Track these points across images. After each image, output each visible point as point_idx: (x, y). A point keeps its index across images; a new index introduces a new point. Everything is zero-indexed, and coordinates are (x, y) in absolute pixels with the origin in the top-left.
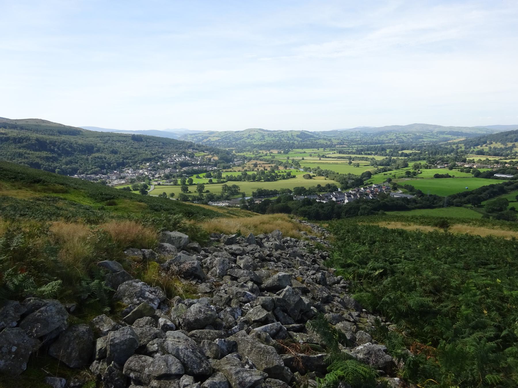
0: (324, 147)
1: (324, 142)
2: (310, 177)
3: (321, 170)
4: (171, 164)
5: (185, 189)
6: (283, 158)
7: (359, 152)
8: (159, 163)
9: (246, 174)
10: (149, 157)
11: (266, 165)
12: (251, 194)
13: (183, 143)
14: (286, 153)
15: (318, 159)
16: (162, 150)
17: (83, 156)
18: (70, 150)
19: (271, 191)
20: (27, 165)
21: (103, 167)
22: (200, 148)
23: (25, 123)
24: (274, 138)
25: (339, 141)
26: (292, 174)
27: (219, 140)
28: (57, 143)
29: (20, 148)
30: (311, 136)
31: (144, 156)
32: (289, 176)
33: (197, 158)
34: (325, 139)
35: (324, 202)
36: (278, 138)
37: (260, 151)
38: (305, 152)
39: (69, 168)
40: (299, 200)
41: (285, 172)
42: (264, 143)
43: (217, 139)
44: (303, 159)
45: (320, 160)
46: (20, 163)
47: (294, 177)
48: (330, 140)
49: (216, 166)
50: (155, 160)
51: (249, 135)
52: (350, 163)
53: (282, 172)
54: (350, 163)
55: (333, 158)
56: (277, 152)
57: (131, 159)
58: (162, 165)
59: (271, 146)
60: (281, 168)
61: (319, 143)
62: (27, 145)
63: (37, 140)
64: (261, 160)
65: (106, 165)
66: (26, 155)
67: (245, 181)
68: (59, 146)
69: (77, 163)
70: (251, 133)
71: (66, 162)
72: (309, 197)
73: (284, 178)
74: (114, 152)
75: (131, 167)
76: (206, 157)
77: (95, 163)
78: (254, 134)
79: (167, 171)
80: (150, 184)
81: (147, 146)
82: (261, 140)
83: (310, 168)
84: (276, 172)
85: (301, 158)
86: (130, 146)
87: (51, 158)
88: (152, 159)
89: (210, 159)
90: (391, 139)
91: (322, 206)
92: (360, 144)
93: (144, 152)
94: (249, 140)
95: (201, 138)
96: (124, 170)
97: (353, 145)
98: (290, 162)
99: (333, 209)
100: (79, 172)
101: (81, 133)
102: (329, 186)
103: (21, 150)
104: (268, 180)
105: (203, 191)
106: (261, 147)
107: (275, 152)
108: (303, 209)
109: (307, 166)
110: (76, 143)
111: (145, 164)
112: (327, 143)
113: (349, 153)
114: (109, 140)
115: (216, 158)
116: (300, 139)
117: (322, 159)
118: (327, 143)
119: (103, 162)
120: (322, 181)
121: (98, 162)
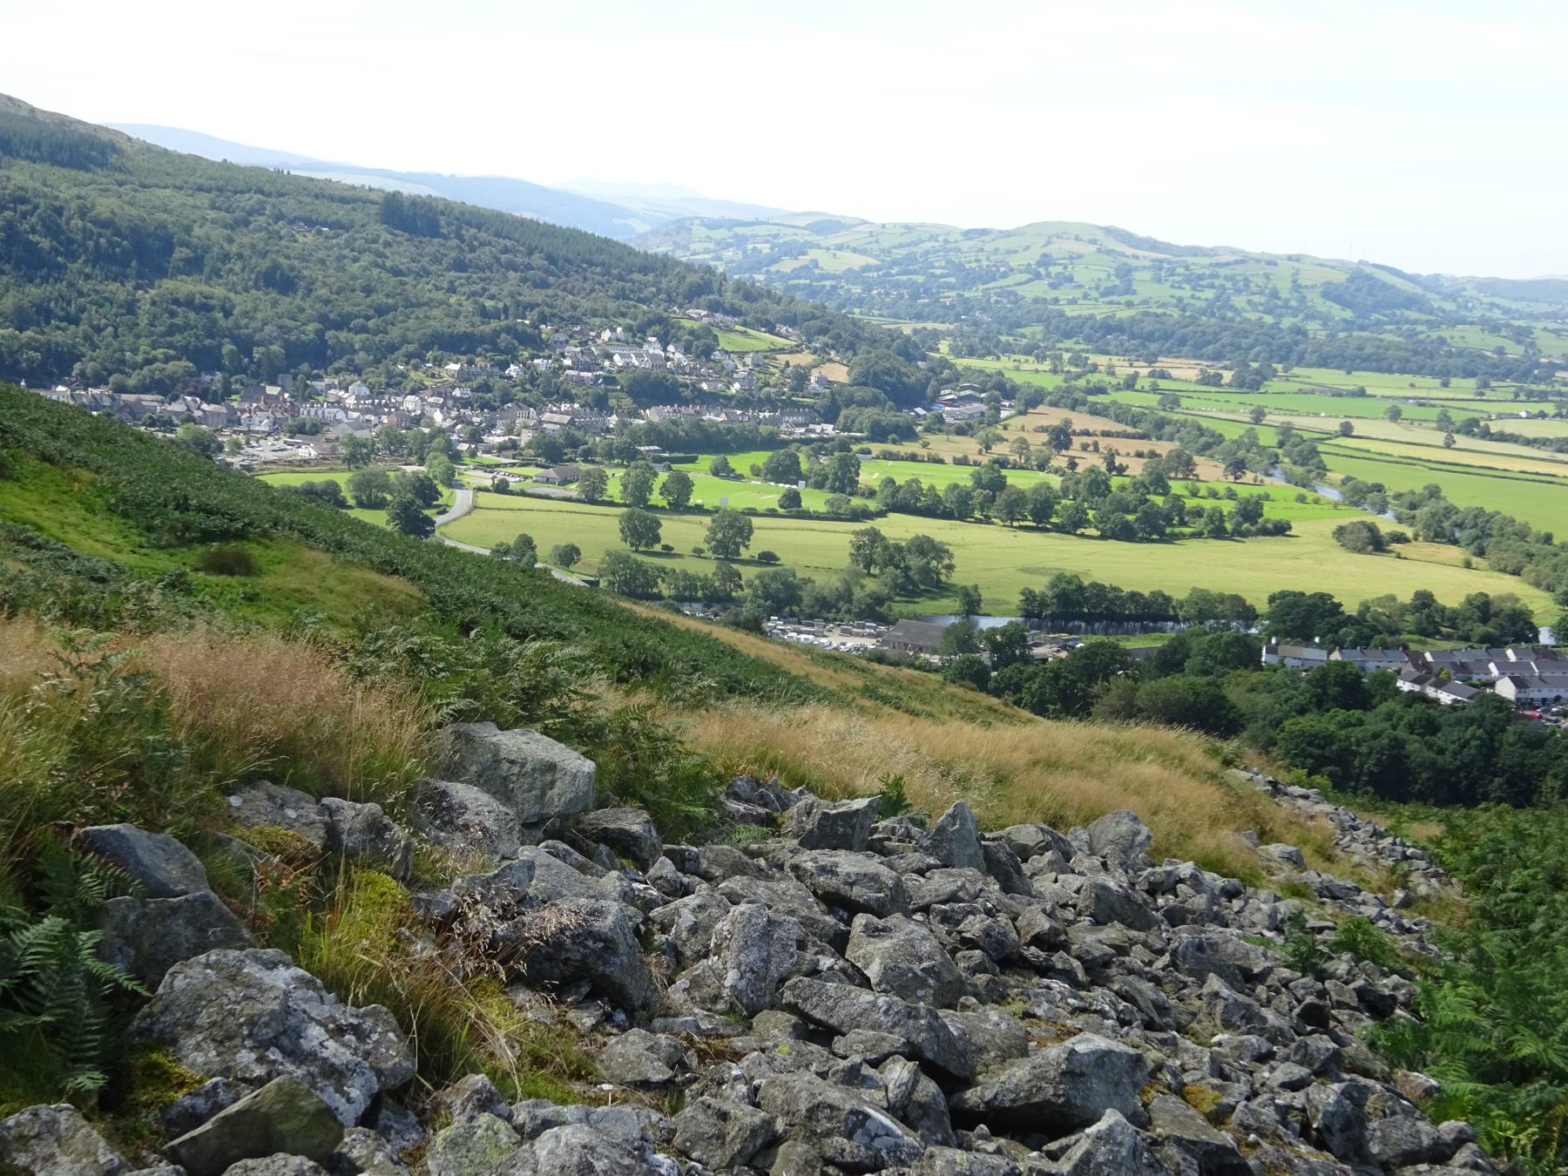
0: (1486, 371)
2: (1377, 543)
3: (1450, 511)
4: (580, 382)
5: (642, 531)
6: (1224, 414)
8: (513, 370)
9: (999, 485)
10: (462, 326)
11: (1125, 446)
12: (1016, 599)
13: (658, 266)
14: (1250, 383)
15: (1440, 438)
16: (539, 296)
17: (114, 286)
18: (45, 243)
19: (1134, 596)
21: (206, 359)
22: (751, 305)
24: (1186, 293)
26: (1271, 513)
27: (867, 268)
30: (1411, 302)
31: (437, 321)
32: (1251, 522)
33: (728, 363)
34: (1495, 329)
35: (1446, 698)
36: (1210, 294)
38: (1361, 393)
39: (28, 346)
40: (1294, 673)
41: (1231, 495)
42: (1123, 314)
43: (858, 261)
44: (1346, 431)
45: (1448, 446)
47: (1281, 529)
48: (1521, 335)
49: (830, 415)
50: (496, 349)
51: (1046, 261)
53: (1214, 495)
55: (1528, 442)
57: (363, 329)
58: (532, 380)
59: (1166, 336)
60: (1211, 472)
64: (1095, 411)
65: (228, 347)
67: (987, 520)
69: (75, 321)
70: (1055, 249)
72: (1355, 657)
73: (1219, 533)
74: (280, 282)
75: (358, 371)
76: (782, 358)
79: (555, 418)
80: (451, 482)
81: (460, 266)
82: (1109, 292)
83: (1379, 488)
84: (1177, 487)
85: (1334, 425)
86: (366, 259)
88: (482, 339)
89: (801, 377)
91: (1429, 721)
93: (440, 295)
94: (1039, 289)
95: (765, 249)
96: (319, 385)
98: (1268, 438)
99: (1490, 748)
100: (82, 374)
101: (113, 159)
102: (1483, 608)
104: (1125, 534)
105: (745, 554)
106: (1104, 334)
107: (1185, 371)
108: (1310, 722)
109: (1367, 474)
110: (83, 213)
111: (439, 362)
112: (1500, 351)
114: (259, 211)
115: (839, 373)
116: (1340, 313)
117: (1461, 441)
118: (1500, 351)
120: (1451, 579)
121: (187, 326)
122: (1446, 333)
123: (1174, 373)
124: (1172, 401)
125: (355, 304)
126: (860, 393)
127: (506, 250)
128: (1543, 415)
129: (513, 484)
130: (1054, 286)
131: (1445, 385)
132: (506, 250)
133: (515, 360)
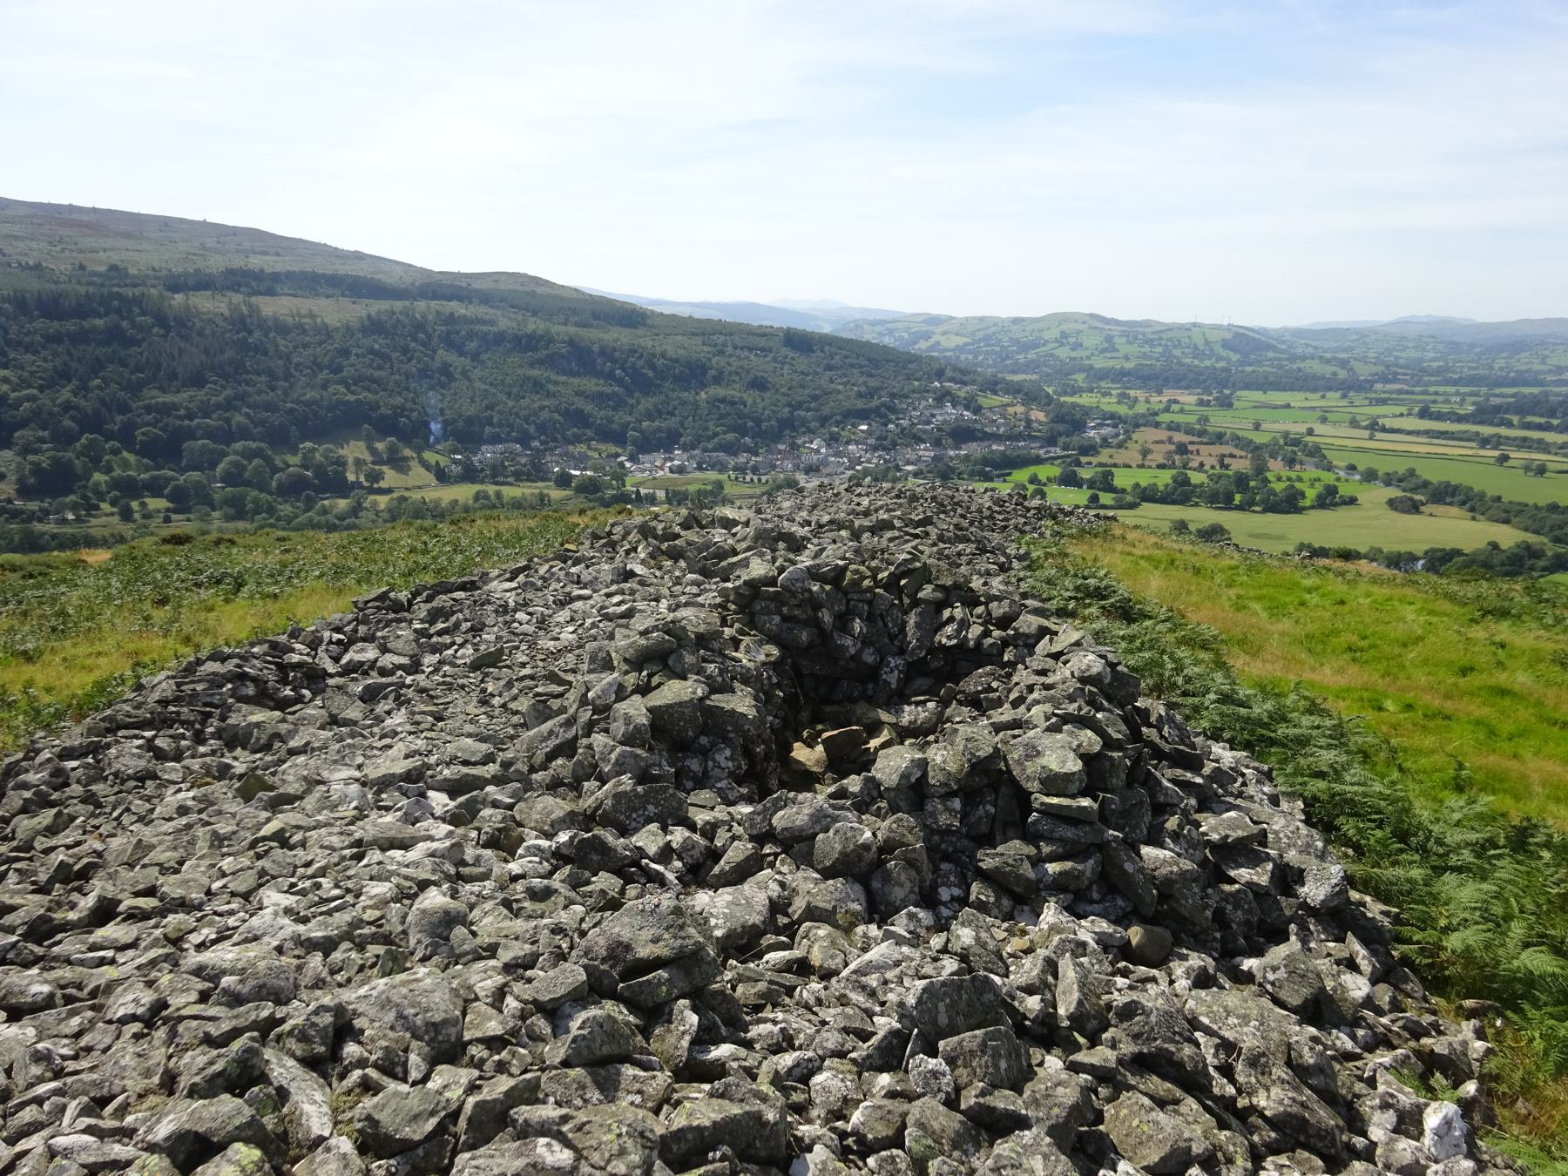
0: (1349, 387)
1: (1327, 370)
2: (1415, 508)
4: (925, 431)
7: (1484, 414)
9: (1186, 482)
10: (860, 404)
14: (1225, 403)
15: (1366, 433)
18: (651, 374)
20: (556, 416)
23: (493, 285)
24: (1147, 349)
25: (1382, 368)
27: (966, 344)
28: (617, 354)
29: (532, 365)
30: (1269, 347)
34: (1328, 361)
36: (1160, 349)
37: (1132, 393)
39: (659, 430)
42: (1129, 365)
43: (961, 341)
44: (1310, 432)
46: (542, 408)
47: (1352, 501)
48: (1343, 364)
49: (1051, 441)
51: (1064, 335)
52: (1504, 459)
54: (1504, 459)
55: (1409, 433)
56: (1193, 399)
57: (808, 410)
59: (1157, 377)
63: (571, 343)
65: (750, 424)
66: (551, 387)
67: (1196, 505)
69: (672, 414)
70: (1064, 327)
71: (647, 410)
74: (759, 385)
76: (1011, 410)
77: (722, 416)
78: (1079, 332)
79: (925, 452)
81: (829, 368)
82: (1104, 351)
85: (1302, 428)
86: (786, 366)
87: (609, 397)
89: (1029, 422)
92: (1455, 383)
94: (1064, 353)
95: (906, 335)
97: (1430, 384)
101: (648, 322)
103: (536, 373)
106: (1120, 376)
107: (1188, 398)
110: (663, 355)
111: (854, 426)
112: (1335, 374)
113: (1460, 419)
114: (724, 345)
115: (1041, 416)
116: (1235, 357)
117: (1379, 435)
118: (1335, 374)
119: (740, 416)
121: (728, 414)
122: (1302, 365)
123: (1181, 399)
124: (1204, 419)
126: (1061, 427)
127: (846, 357)
131: (1323, 397)
132: (846, 357)
133: (890, 421)
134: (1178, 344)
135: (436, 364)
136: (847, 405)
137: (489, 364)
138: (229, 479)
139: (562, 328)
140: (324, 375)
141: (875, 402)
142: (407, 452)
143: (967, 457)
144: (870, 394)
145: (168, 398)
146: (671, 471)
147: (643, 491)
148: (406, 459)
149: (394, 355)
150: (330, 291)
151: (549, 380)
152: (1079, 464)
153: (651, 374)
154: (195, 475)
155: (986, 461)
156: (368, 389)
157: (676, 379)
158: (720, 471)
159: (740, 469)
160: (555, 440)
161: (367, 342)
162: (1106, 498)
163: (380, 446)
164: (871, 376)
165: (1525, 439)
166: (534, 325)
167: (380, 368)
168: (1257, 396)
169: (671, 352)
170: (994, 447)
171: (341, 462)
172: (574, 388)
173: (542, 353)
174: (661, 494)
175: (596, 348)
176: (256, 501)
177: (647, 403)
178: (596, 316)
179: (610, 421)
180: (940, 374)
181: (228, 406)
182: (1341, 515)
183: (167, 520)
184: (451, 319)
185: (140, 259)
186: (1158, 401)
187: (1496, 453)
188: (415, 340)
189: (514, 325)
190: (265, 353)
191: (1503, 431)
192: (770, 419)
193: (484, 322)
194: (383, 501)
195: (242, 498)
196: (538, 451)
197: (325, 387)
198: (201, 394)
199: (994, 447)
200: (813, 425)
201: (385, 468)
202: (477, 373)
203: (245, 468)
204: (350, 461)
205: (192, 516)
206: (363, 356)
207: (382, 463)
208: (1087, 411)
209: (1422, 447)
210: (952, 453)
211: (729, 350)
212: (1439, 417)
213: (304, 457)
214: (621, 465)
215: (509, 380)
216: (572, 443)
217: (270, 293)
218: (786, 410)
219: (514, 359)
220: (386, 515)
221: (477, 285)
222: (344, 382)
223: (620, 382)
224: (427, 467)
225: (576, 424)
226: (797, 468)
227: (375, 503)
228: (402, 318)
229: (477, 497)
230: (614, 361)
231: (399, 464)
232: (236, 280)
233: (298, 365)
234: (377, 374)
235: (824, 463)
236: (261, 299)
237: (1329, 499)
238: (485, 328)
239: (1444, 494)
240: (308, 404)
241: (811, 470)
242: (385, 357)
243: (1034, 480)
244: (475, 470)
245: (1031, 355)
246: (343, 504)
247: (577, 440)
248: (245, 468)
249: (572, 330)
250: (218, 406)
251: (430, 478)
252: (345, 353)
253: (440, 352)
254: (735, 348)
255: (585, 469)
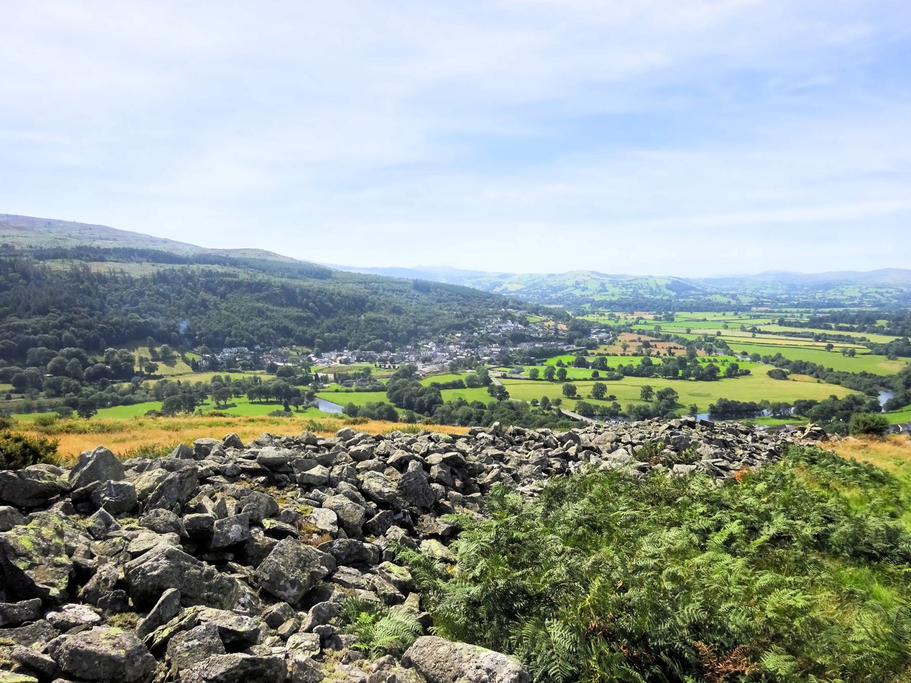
0: (738, 309)
1: (725, 300)
2: (784, 376)
4: (496, 337)
7: (815, 323)
10: (457, 321)
12: (708, 408)
14: (670, 319)
15: (751, 334)
18: (331, 305)
19: (744, 403)
20: (271, 330)
21: (387, 339)
23: (242, 256)
24: (624, 290)
29: (258, 301)
30: (692, 288)
34: (725, 295)
36: (631, 290)
37: (617, 314)
38: (705, 320)
39: (335, 338)
42: (614, 299)
43: (519, 287)
44: (719, 334)
46: (262, 326)
47: (747, 373)
48: (734, 297)
49: (570, 341)
51: (577, 283)
52: (830, 347)
54: (830, 347)
56: (651, 317)
57: (426, 325)
59: (630, 305)
61: (714, 301)
62: (267, 295)
63: (283, 287)
65: (391, 334)
66: (269, 313)
67: (657, 377)
68: (316, 297)
69: (344, 329)
70: (577, 279)
71: (328, 326)
74: (397, 311)
76: (546, 324)
77: (373, 330)
79: (496, 349)
81: (440, 301)
82: (600, 291)
85: (714, 332)
87: (304, 319)
88: (463, 325)
89: (557, 330)
90: (852, 298)
92: (796, 306)
94: (578, 293)
95: (488, 284)
97: (782, 307)
101: (333, 275)
103: (260, 305)
105: (605, 396)
106: (610, 305)
107: (649, 317)
110: (339, 294)
111: (453, 334)
112: (729, 302)
113: (802, 326)
114: (378, 289)
115: (564, 327)
117: (758, 335)
118: (729, 302)
121: (377, 328)
122: (710, 298)
123: (644, 317)
124: (658, 328)
125: (423, 316)
126: (576, 333)
128: (769, 324)
129: (508, 375)
130: (583, 291)
131: (724, 315)
133: (475, 331)
134: (641, 287)
135: (198, 301)
136: (449, 322)
137: (232, 299)
138: (55, 371)
139: (277, 279)
140: (127, 307)
141: (466, 320)
142: (175, 353)
143: (520, 352)
144: (464, 315)
145: (22, 322)
146: (341, 362)
147: (320, 375)
148: (174, 357)
149: (172, 295)
150: (141, 259)
151: (268, 309)
152: (587, 354)
153: (331, 305)
154: (32, 370)
155: (531, 353)
156: (154, 316)
157: (346, 308)
158: (371, 362)
159: (383, 361)
160: (270, 344)
161: (155, 287)
162: (603, 374)
163: (158, 349)
164: (464, 305)
165: (840, 336)
166: (261, 277)
167: (162, 302)
168: (687, 315)
169: (344, 292)
170: (537, 345)
171: (131, 360)
172: (284, 314)
173: (264, 294)
174: (331, 376)
175: (298, 290)
176: (67, 385)
177: (328, 322)
178: (300, 272)
179: (304, 333)
180: (505, 304)
181: (61, 326)
182: (742, 380)
183: (9, 398)
184: (209, 274)
185: (23, 241)
186: (631, 318)
187: (826, 344)
188: (186, 286)
189: (248, 277)
190: (90, 294)
191: (828, 332)
192: (403, 330)
193: (230, 275)
194: (152, 383)
195: (59, 383)
196: (258, 351)
197: (125, 315)
198: (44, 319)
199: (537, 345)
200: (429, 334)
201: (159, 363)
202: (224, 305)
203: (65, 364)
204: (137, 359)
205: (25, 395)
206: (152, 295)
207: (158, 360)
208: (591, 324)
209: (783, 341)
210: (511, 349)
211: (381, 291)
212: (790, 324)
213: (107, 357)
214: (310, 359)
215: (243, 309)
216: (281, 347)
217: (102, 260)
218: (413, 325)
219: (247, 297)
220: (152, 392)
221: (232, 256)
222: (138, 311)
223: (311, 310)
224: (186, 361)
225: (286, 335)
226: (418, 359)
227: (147, 385)
228: (178, 273)
229: (214, 379)
230: (309, 298)
231: (169, 360)
232: (83, 253)
233: (110, 301)
234: (159, 306)
235: (435, 356)
236: (95, 263)
237: (734, 372)
238: (230, 279)
239: (800, 368)
240: (113, 324)
241: (427, 360)
242: (166, 296)
243: (560, 364)
244: (218, 363)
245: (559, 294)
246: (126, 386)
247: (283, 344)
248: (65, 364)
249: (284, 280)
250: (55, 326)
251: (188, 369)
252: (141, 294)
253: (201, 293)
254: (384, 290)
255: (287, 362)
